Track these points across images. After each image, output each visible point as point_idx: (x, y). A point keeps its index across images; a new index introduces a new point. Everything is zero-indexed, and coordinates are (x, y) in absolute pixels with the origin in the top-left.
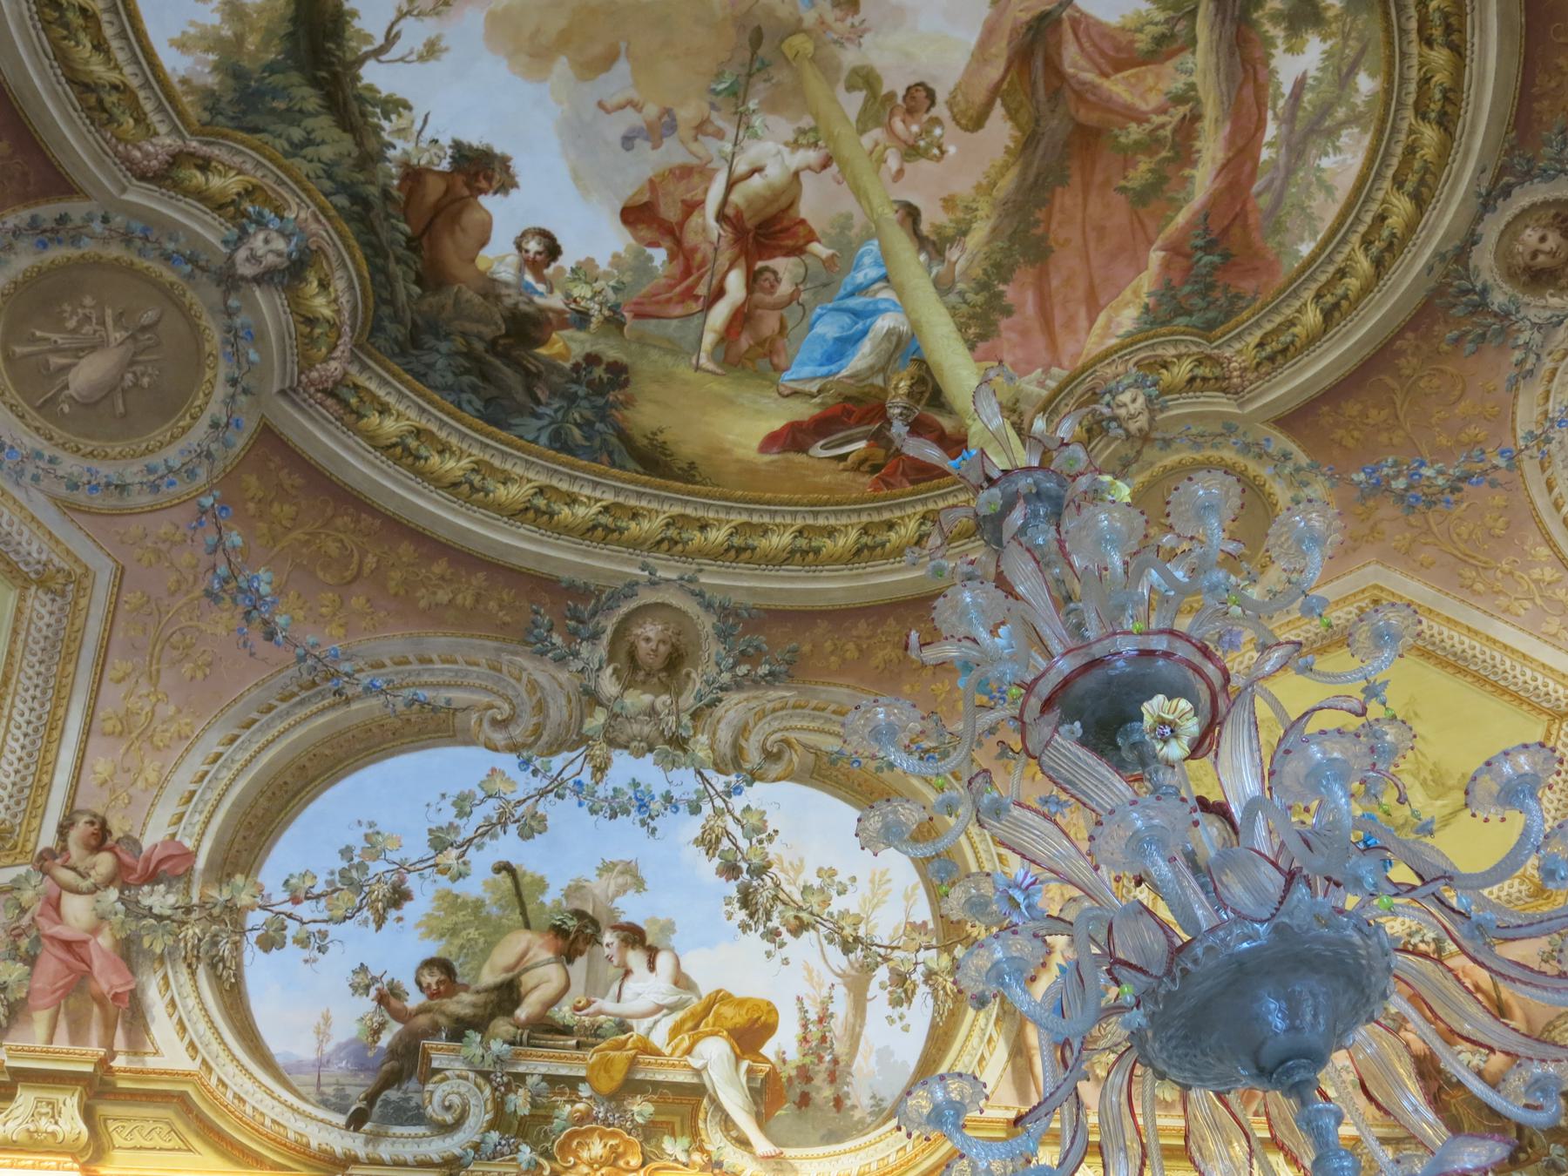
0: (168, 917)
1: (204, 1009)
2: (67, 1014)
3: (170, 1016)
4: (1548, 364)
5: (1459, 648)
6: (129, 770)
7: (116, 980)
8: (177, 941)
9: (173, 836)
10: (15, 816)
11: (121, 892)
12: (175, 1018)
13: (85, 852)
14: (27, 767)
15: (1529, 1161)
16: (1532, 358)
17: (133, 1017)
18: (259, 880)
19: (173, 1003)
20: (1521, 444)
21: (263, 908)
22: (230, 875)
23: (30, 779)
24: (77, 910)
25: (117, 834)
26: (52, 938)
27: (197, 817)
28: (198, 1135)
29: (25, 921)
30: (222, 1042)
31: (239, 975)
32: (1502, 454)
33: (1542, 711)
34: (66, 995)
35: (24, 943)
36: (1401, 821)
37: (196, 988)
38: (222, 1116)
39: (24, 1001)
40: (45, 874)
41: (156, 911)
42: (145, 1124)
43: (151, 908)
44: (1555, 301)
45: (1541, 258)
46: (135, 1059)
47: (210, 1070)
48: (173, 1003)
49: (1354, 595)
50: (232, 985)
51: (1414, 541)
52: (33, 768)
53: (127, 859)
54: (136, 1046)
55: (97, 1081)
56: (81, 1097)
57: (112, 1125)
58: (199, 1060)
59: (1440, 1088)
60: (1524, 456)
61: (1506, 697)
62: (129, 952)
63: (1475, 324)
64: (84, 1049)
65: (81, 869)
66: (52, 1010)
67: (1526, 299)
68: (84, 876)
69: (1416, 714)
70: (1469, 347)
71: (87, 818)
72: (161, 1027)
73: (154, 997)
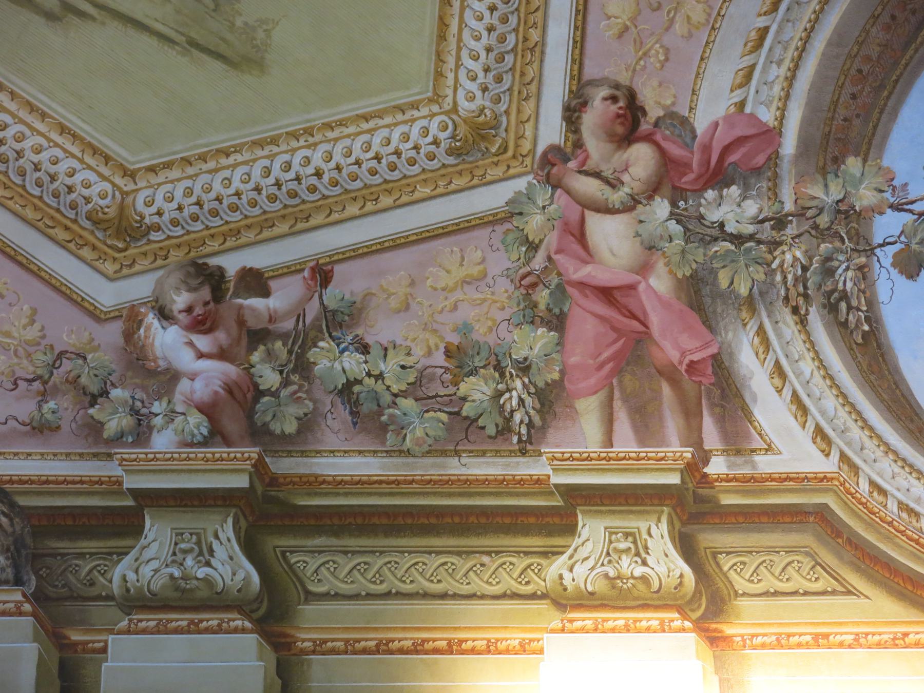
0: (751, 237)
1: (829, 376)
2: (625, 399)
3: (779, 391)
6: (659, 7)
7: (688, 342)
8: (771, 273)
9: (741, 105)
10: (497, 100)
11: (674, 204)
12: (787, 393)
13: (610, 147)
14: (504, 20)
17: (723, 396)
18: (886, 163)
19: (779, 371)
21: (897, 208)
22: (838, 161)
23: (511, 39)
24: (612, 237)
25: (654, 112)
26: (582, 285)
27: (774, 71)
28: (858, 570)
29: (538, 262)
30: (866, 425)
31: (873, 318)
34: (618, 371)
35: (543, 296)
37: (812, 345)
38: (888, 538)
39: (558, 385)
40: (555, 187)
41: (730, 228)
42: (775, 558)
43: (722, 225)
46: (739, 460)
47: (855, 469)
48: (779, 371)
50: (865, 335)
52: (513, 20)
53: (675, 151)
54: (736, 446)
55: (690, 499)
56: (671, 523)
57: (726, 563)
58: (835, 456)
62: (699, 296)
64: (661, 451)
65: (607, 174)
66: (606, 390)
68: (613, 184)
71: (604, 92)
72: (769, 410)
73: (748, 362)
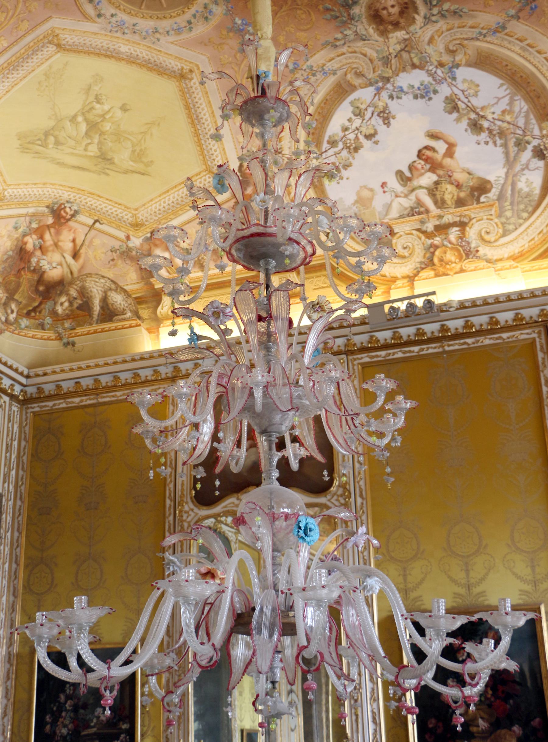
4: (344, 49)
5: (201, 115)
15: (34, 318)
16: (342, 42)
20: (305, 67)
32: (295, 64)
33: (205, 164)
36: (109, 157)
44: (371, 31)
45: (385, 12)
49: (186, 61)
51: (230, 63)
59: (24, 268)
60: (301, 72)
61: (198, 148)
63: (339, 11)
67: (364, 20)
69: (159, 124)
70: (328, 16)
